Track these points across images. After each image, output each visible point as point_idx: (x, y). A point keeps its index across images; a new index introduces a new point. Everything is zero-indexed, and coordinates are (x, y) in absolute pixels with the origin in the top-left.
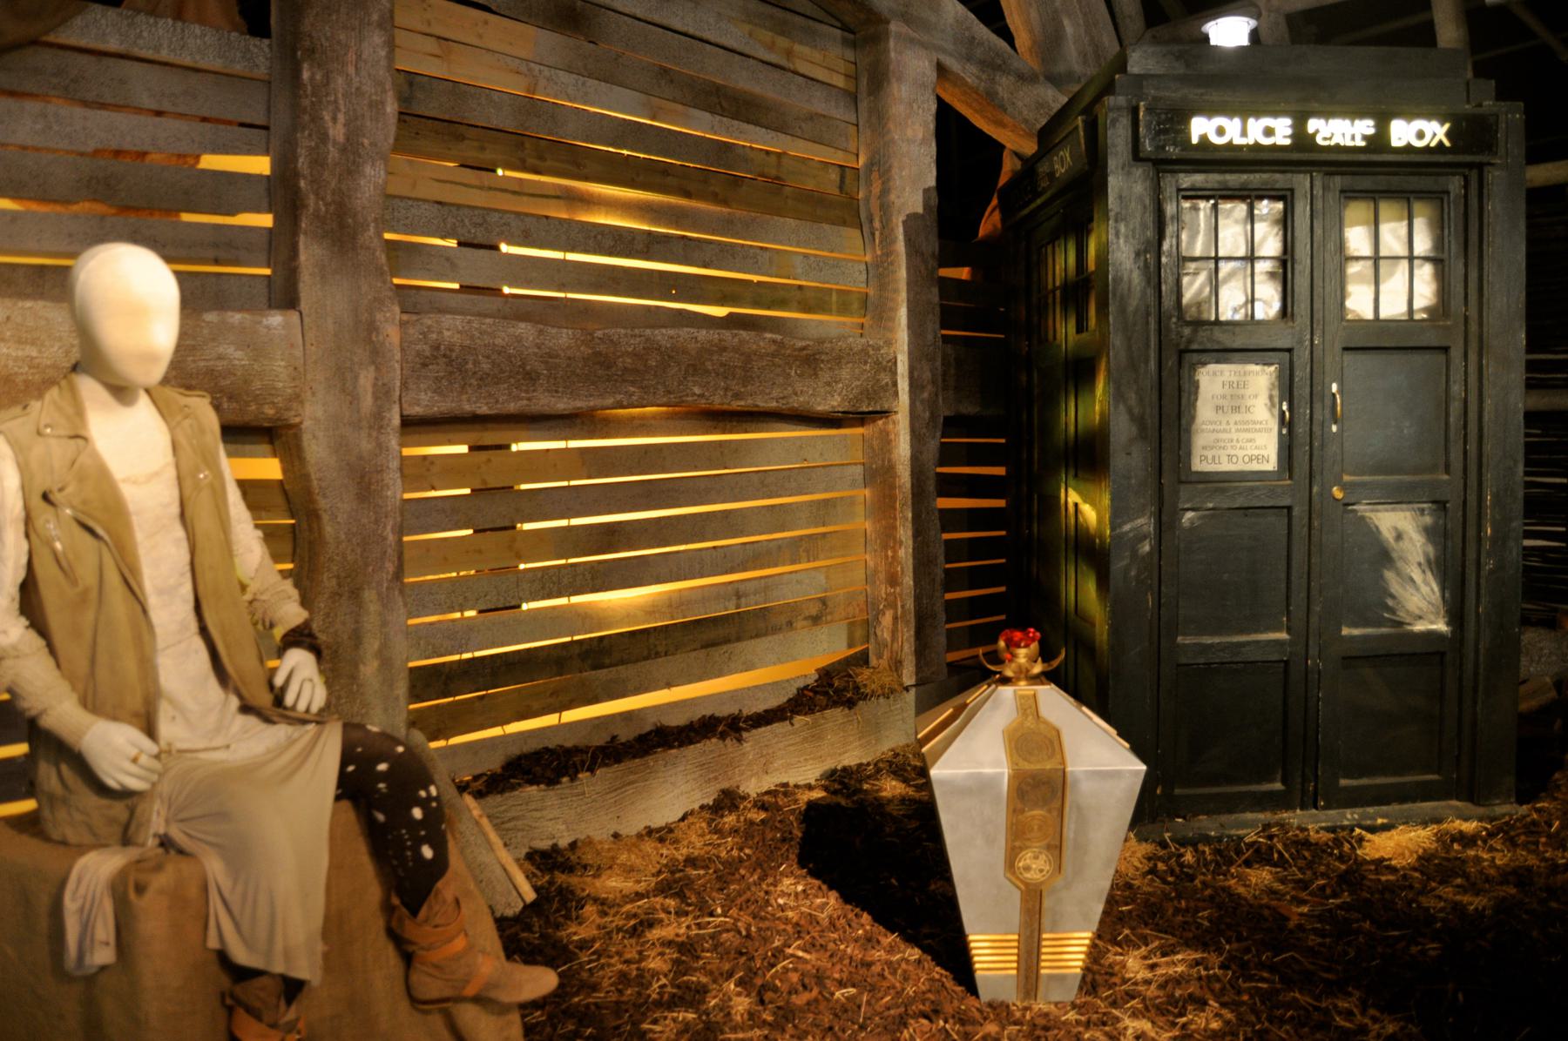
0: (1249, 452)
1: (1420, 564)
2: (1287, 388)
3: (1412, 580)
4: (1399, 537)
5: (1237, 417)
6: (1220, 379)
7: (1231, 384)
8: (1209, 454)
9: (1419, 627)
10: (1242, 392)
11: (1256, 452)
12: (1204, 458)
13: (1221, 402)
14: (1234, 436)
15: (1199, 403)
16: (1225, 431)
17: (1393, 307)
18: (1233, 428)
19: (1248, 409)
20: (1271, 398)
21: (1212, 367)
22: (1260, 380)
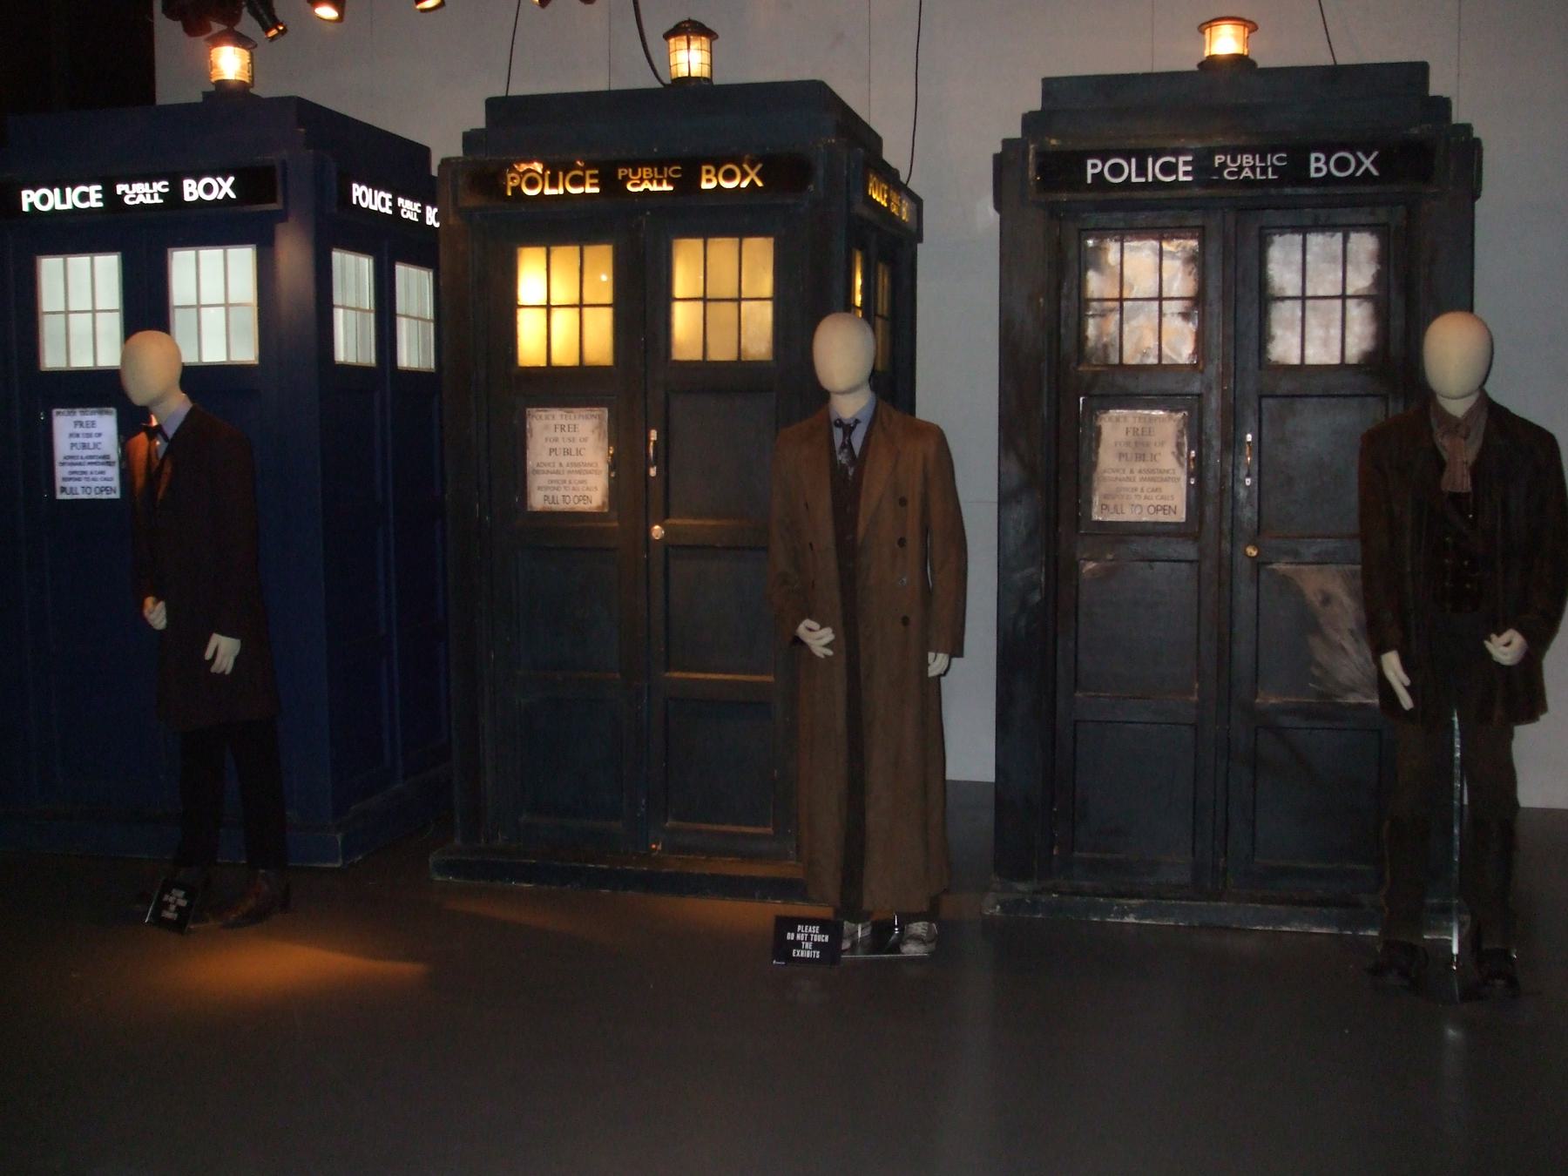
0: (1156, 502)
1: (1352, 632)
2: (1195, 434)
3: (1343, 648)
4: (1327, 600)
5: (1142, 465)
6: (1122, 426)
7: (1135, 431)
8: (1111, 503)
9: (1352, 699)
10: (1147, 439)
11: (1162, 503)
12: (1104, 507)
13: (1125, 449)
14: (1139, 485)
15: (1101, 450)
16: (1129, 479)
17: (1322, 352)
18: (1138, 476)
19: (1153, 457)
20: (1179, 446)
21: (1114, 413)
22: (1164, 425)
